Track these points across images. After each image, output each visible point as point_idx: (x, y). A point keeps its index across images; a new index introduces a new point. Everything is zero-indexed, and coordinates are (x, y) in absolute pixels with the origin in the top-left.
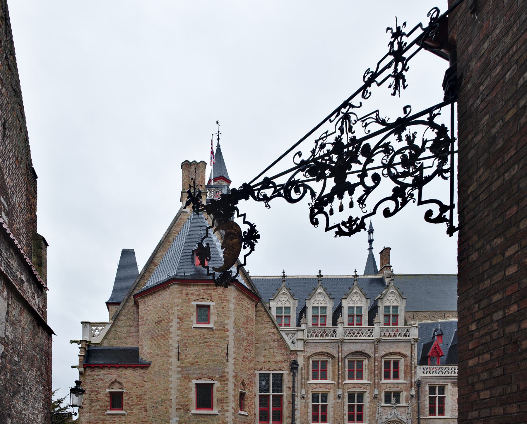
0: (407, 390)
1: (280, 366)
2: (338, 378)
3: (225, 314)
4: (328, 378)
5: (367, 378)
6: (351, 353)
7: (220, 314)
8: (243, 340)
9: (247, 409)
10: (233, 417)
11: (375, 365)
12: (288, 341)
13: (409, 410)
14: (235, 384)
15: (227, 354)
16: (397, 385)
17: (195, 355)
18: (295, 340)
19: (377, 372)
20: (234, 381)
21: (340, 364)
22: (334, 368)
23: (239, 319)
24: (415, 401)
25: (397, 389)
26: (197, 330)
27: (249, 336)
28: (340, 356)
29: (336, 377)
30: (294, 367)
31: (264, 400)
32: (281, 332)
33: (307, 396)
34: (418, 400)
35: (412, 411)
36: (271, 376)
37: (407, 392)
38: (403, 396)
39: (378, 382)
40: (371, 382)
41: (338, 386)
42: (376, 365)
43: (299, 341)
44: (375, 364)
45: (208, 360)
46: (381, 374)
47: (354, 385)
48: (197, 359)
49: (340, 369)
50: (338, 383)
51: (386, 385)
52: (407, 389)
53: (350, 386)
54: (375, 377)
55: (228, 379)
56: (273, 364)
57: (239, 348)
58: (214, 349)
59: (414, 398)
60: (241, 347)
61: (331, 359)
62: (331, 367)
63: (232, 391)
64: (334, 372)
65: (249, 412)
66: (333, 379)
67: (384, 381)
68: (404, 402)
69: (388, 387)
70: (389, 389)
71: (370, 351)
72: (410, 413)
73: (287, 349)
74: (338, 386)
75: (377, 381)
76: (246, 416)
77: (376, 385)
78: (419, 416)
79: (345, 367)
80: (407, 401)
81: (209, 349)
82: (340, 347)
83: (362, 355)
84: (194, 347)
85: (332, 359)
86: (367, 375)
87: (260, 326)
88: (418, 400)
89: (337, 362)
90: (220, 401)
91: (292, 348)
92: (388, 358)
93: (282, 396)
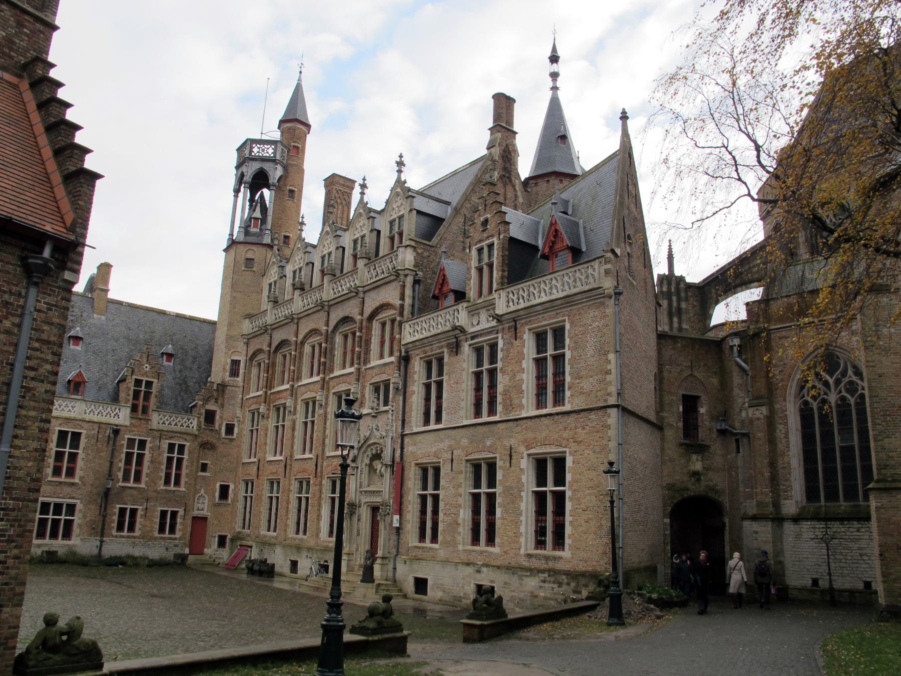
33: (295, 408)
34: (405, 393)
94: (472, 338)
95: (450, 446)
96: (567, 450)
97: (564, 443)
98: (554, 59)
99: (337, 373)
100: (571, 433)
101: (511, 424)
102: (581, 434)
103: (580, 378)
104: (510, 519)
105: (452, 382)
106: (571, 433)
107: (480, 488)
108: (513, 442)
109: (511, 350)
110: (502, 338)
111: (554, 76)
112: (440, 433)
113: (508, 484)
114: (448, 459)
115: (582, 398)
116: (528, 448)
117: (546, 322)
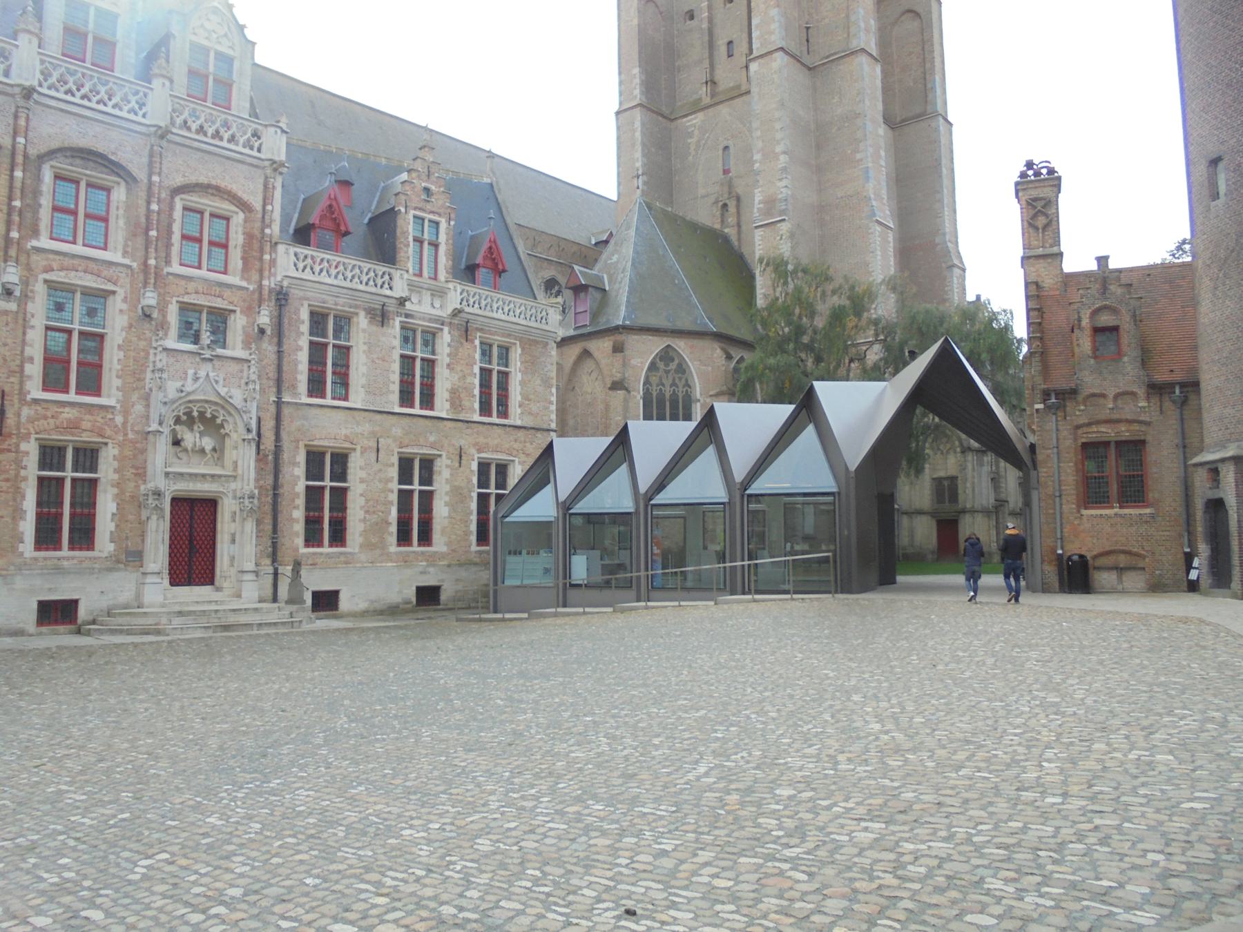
0: (250, 311)
5: (120, 247)
11: (148, 209)
13: (252, 371)
16: (218, 289)
19: (153, 233)
21: (18, 174)
24: (270, 348)
25: (219, 303)
28: (20, 147)
34: (280, 344)
35: (259, 377)
37: (247, 316)
38: (238, 324)
39: (156, 267)
40: (135, 265)
41: (6, 252)
42: (153, 211)
44: (148, 209)
46: (169, 245)
47: (71, 261)
49: (18, 193)
51: (183, 283)
52: (250, 308)
53: (54, 260)
54: (147, 248)
59: (266, 338)
68: (240, 345)
69: (189, 290)
70: (194, 296)
71: (137, 165)
72: (254, 381)
74: (6, 252)
75: (152, 262)
78: (279, 392)
79: (37, 193)
80: (247, 345)
82: (23, 116)
83: (106, 167)
88: (280, 344)
94: (407, 316)
95: (373, 433)
96: (517, 460)
97: (515, 453)
99: (44, 242)
100: (521, 445)
101: (460, 424)
103: (529, 400)
104: (459, 518)
105: (375, 356)
106: (521, 445)
107: (488, 487)
108: (462, 442)
109: (461, 350)
110: (450, 333)
112: (356, 413)
113: (456, 484)
114: (370, 447)
116: (479, 451)
117: (498, 339)
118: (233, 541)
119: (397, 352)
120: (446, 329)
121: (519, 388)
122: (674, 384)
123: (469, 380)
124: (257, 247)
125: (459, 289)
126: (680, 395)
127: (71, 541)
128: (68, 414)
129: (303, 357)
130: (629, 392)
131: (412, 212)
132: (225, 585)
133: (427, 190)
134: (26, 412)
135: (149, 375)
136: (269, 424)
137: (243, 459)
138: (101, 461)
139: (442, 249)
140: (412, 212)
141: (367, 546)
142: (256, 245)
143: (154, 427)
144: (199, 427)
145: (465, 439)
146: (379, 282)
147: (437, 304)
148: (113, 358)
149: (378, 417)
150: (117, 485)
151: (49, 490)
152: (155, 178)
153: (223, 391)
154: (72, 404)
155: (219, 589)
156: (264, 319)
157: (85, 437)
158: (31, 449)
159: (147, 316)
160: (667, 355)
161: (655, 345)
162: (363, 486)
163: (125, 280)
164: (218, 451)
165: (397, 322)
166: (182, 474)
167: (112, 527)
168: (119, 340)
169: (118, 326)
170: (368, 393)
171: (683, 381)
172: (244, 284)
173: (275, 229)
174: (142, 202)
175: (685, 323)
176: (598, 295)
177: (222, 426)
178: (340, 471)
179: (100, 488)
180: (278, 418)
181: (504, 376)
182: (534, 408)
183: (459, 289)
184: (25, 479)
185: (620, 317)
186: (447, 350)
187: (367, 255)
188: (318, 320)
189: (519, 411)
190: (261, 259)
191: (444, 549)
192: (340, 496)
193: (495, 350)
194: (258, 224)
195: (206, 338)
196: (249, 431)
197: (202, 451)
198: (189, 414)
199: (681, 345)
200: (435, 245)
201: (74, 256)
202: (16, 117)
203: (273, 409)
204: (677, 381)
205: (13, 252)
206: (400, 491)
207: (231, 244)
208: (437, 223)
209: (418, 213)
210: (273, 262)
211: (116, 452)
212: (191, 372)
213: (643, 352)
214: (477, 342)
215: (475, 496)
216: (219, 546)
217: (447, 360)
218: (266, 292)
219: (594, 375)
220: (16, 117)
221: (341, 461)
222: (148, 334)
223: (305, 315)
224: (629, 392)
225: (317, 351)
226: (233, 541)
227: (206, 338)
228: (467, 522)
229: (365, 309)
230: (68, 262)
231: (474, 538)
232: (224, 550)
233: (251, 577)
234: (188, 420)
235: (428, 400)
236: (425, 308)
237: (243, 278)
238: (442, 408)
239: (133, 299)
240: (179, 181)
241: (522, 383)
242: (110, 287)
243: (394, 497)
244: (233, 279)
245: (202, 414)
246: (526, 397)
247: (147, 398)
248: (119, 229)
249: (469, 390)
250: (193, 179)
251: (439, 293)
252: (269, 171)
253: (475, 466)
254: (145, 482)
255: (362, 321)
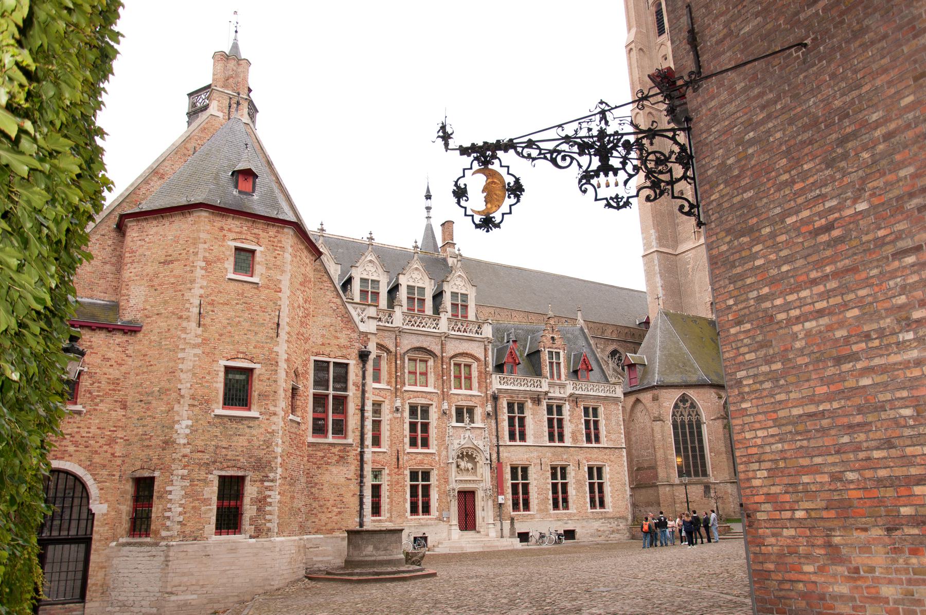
1: (345, 352)
2: (396, 382)
3: (276, 267)
4: (382, 381)
6: (415, 348)
7: (271, 266)
8: (299, 307)
9: (299, 414)
10: (282, 424)
11: (443, 368)
12: (357, 319)
14: (287, 372)
15: (278, 325)
17: (228, 321)
18: (366, 318)
19: (445, 378)
20: (286, 367)
21: (398, 362)
22: (390, 368)
23: (295, 277)
25: (471, 404)
26: (233, 283)
27: (306, 303)
29: (393, 380)
30: (363, 356)
31: (320, 400)
32: (347, 304)
34: (496, 419)
36: (331, 366)
38: (479, 413)
43: (371, 320)
44: (443, 368)
45: (248, 330)
46: (451, 381)
48: (229, 328)
50: (396, 389)
52: (483, 404)
55: (277, 362)
56: (335, 349)
57: (293, 319)
58: (258, 315)
60: (296, 317)
61: (385, 354)
62: (386, 366)
63: (283, 384)
64: (390, 373)
65: (303, 418)
66: (389, 383)
67: (454, 391)
71: (436, 349)
73: (355, 328)
75: (445, 390)
76: (299, 423)
77: (444, 396)
78: (498, 441)
79: (404, 367)
80: (483, 421)
81: (250, 314)
84: (226, 308)
85: (387, 354)
86: (433, 382)
87: (318, 292)
88: (496, 419)
89: (394, 359)
90: (263, 396)
91: (363, 328)
92: (459, 360)
93: (346, 397)
94: (549, 399)
98: (428, 197)
99: (407, 388)
102: (613, 458)
108: (579, 457)
111: (428, 208)
115: (611, 442)
116: (588, 461)
117: (591, 404)
118: (483, 510)
119: (546, 417)
120: (567, 403)
121: (604, 428)
122: (689, 415)
123: (579, 427)
124: (484, 376)
125: (571, 383)
126: (694, 420)
127: (423, 512)
128: (420, 457)
129: (505, 425)
130: (664, 422)
131: (547, 350)
132: (481, 530)
133: (553, 338)
134: (405, 458)
135: (447, 438)
136: (494, 456)
137: (485, 470)
138: (431, 477)
139: (562, 365)
140: (547, 350)
141: (540, 510)
142: (483, 376)
143: (451, 461)
144: (466, 459)
145: (581, 456)
146: (536, 385)
147: (562, 391)
148: (433, 432)
149: (540, 448)
150: (438, 487)
151: (414, 489)
152: (444, 354)
153: (475, 443)
154: (420, 453)
155: (479, 532)
156: (489, 408)
157: (426, 467)
158: (407, 472)
159: (445, 413)
160: (684, 399)
161: (676, 394)
162: (536, 482)
163: (436, 399)
164: (474, 469)
165: (544, 403)
166: (461, 481)
167: (437, 505)
168: (435, 424)
169: (434, 419)
170: (535, 437)
171: (695, 413)
172: (479, 394)
173: (490, 368)
174: (440, 365)
175: (693, 379)
176: (641, 368)
177: (475, 458)
178: (525, 476)
179: (431, 488)
180: (498, 453)
181: (596, 423)
182: (613, 437)
183: (571, 383)
184: (406, 486)
185: (656, 379)
186: (569, 413)
187: (531, 375)
188: (510, 406)
189: (605, 439)
190: (486, 382)
191: (575, 511)
192: (526, 487)
193: (591, 410)
194: (483, 367)
195: (467, 419)
196: (487, 459)
197: (468, 469)
198: (462, 454)
199: (692, 393)
200: (558, 364)
201: (417, 392)
202: (396, 339)
203: (496, 449)
204: (691, 413)
205: (398, 394)
206: (552, 483)
207: (473, 376)
208: (559, 353)
209: (550, 350)
210: (491, 382)
211: (436, 472)
212: (462, 435)
213: (670, 398)
214: (582, 408)
215: (587, 484)
216: (477, 512)
217: (569, 418)
218: (489, 396)
219: (644, 412)
220: (396, 339)
221: (525, 470)
222: (446, 421)
223: (505, 405)
224: (664, 422)
225: (511, 420)
226: (483, 510)
227: (467, 419)
228: (585, 497)
229: (530, 398)
230: (416, 394)
231: (589, 505)
232: (479, 513)
233: (492, 526)
234: (461, 456)
235: (561, 438)
236: (557, 395)
237: (479, 391)
238: (568, 442)
239: (439, 407)
240: (452, 353)
241: (606, 425)
242: (431, 402)
243: (550, 486)
244: (474, 392)
245: (467, 453)
246: (608, 432)
247: (447, 448)
248: (431, 378)
249: (580, 431)
250: (457, 352)
251: (562, 386)
252: (486, 343)
253: (586, 469)
254: (448, 485)
255: (529, 404)
